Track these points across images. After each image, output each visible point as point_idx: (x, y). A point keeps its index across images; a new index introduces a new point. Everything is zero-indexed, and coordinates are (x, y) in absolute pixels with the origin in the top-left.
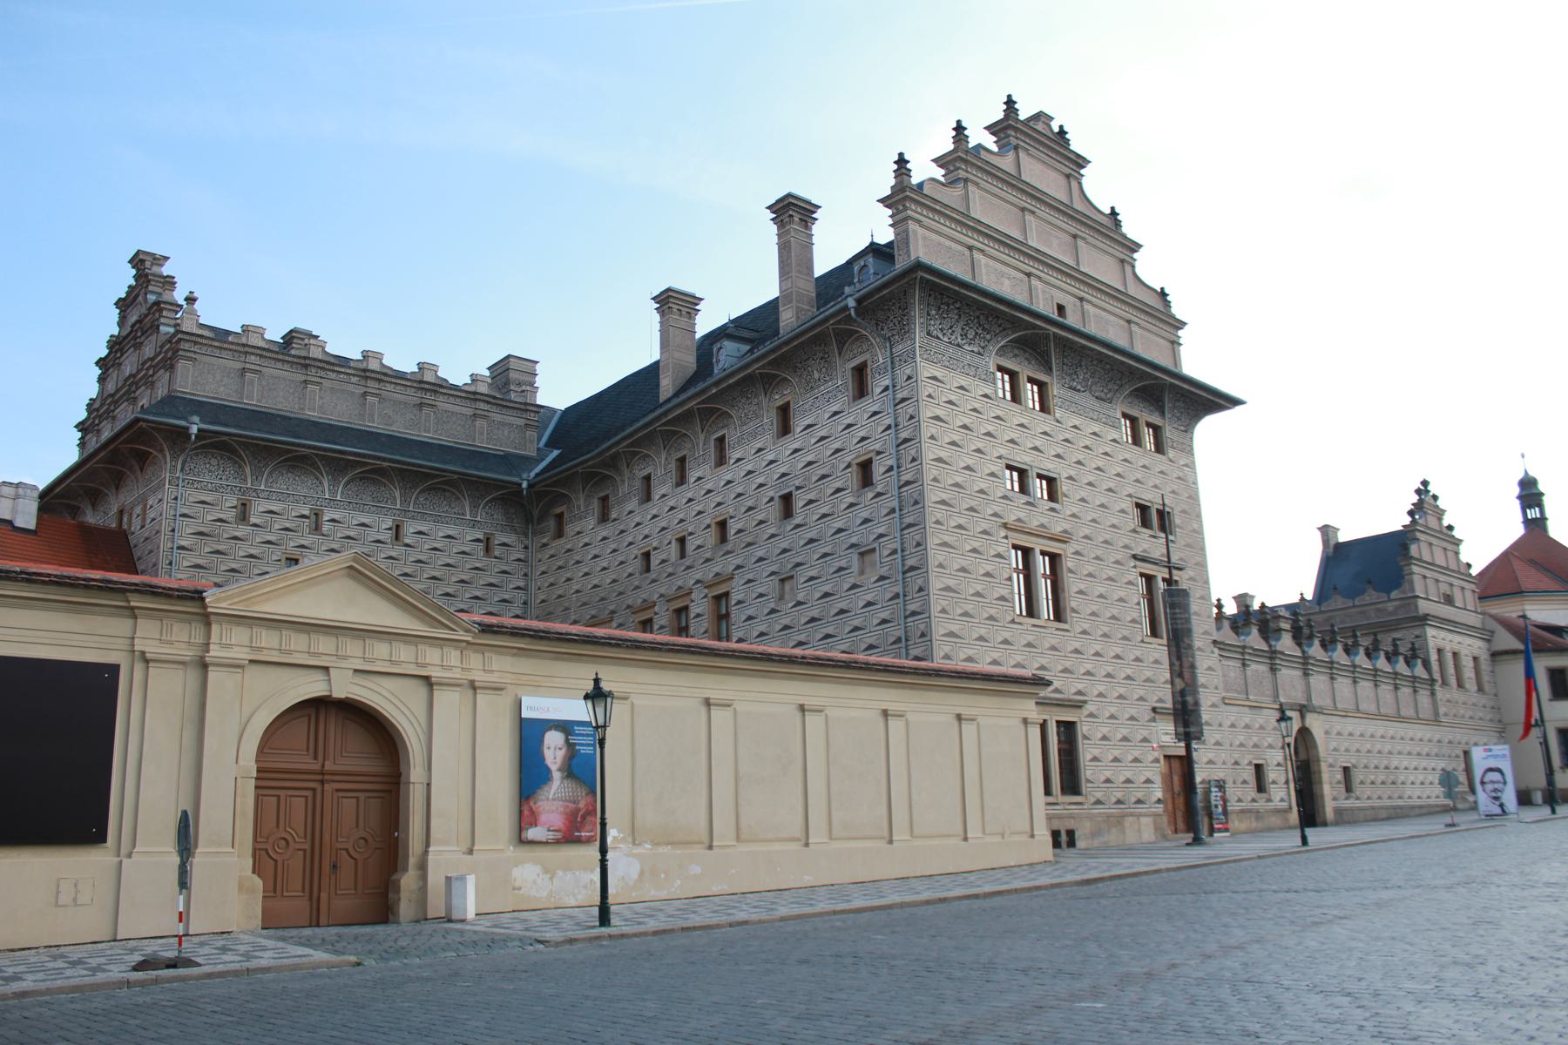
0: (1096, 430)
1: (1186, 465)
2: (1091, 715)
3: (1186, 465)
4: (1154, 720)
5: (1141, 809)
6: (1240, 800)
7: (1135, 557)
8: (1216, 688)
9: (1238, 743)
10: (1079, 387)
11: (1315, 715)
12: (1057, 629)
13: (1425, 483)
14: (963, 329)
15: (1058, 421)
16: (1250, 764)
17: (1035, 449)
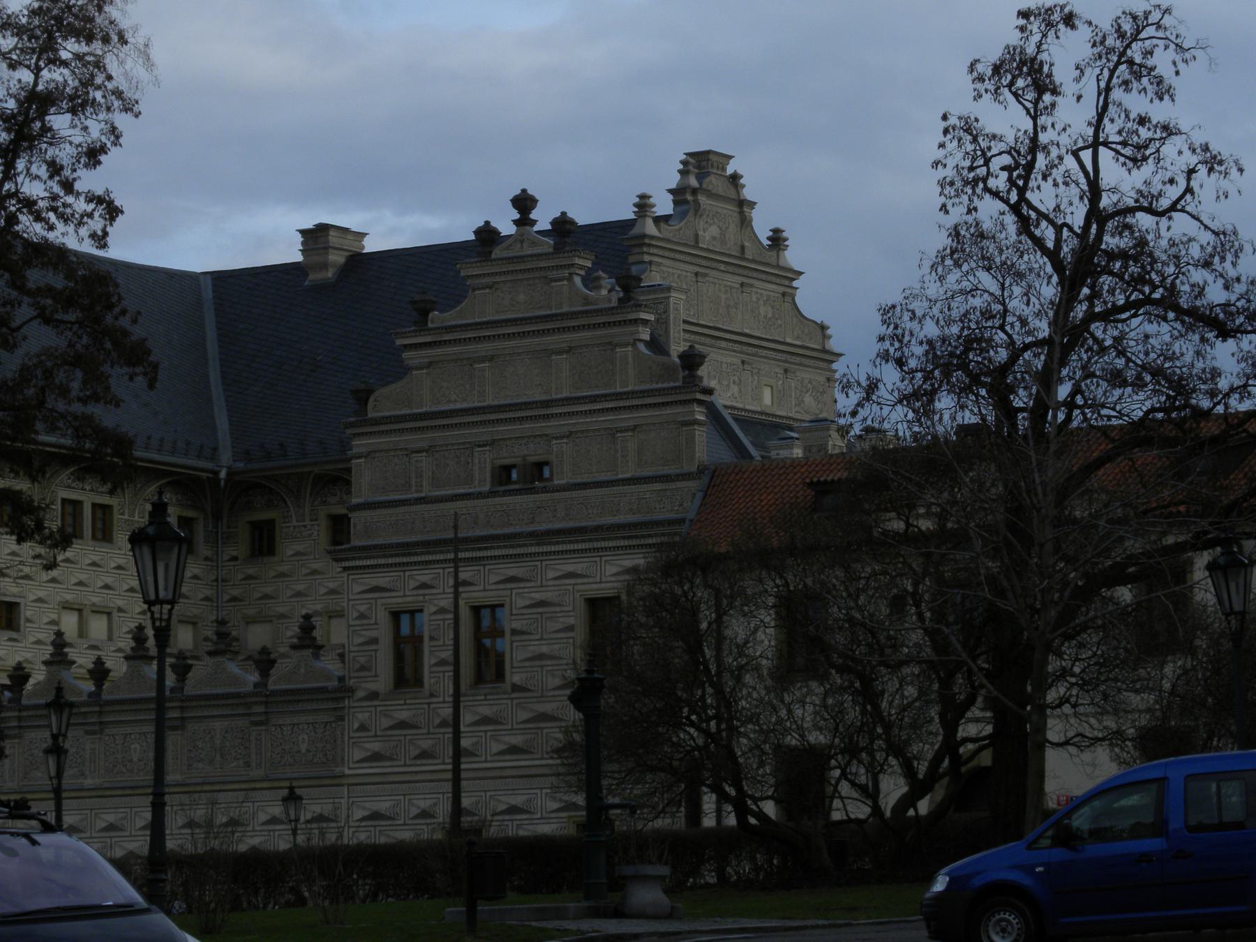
13: (524, 203)
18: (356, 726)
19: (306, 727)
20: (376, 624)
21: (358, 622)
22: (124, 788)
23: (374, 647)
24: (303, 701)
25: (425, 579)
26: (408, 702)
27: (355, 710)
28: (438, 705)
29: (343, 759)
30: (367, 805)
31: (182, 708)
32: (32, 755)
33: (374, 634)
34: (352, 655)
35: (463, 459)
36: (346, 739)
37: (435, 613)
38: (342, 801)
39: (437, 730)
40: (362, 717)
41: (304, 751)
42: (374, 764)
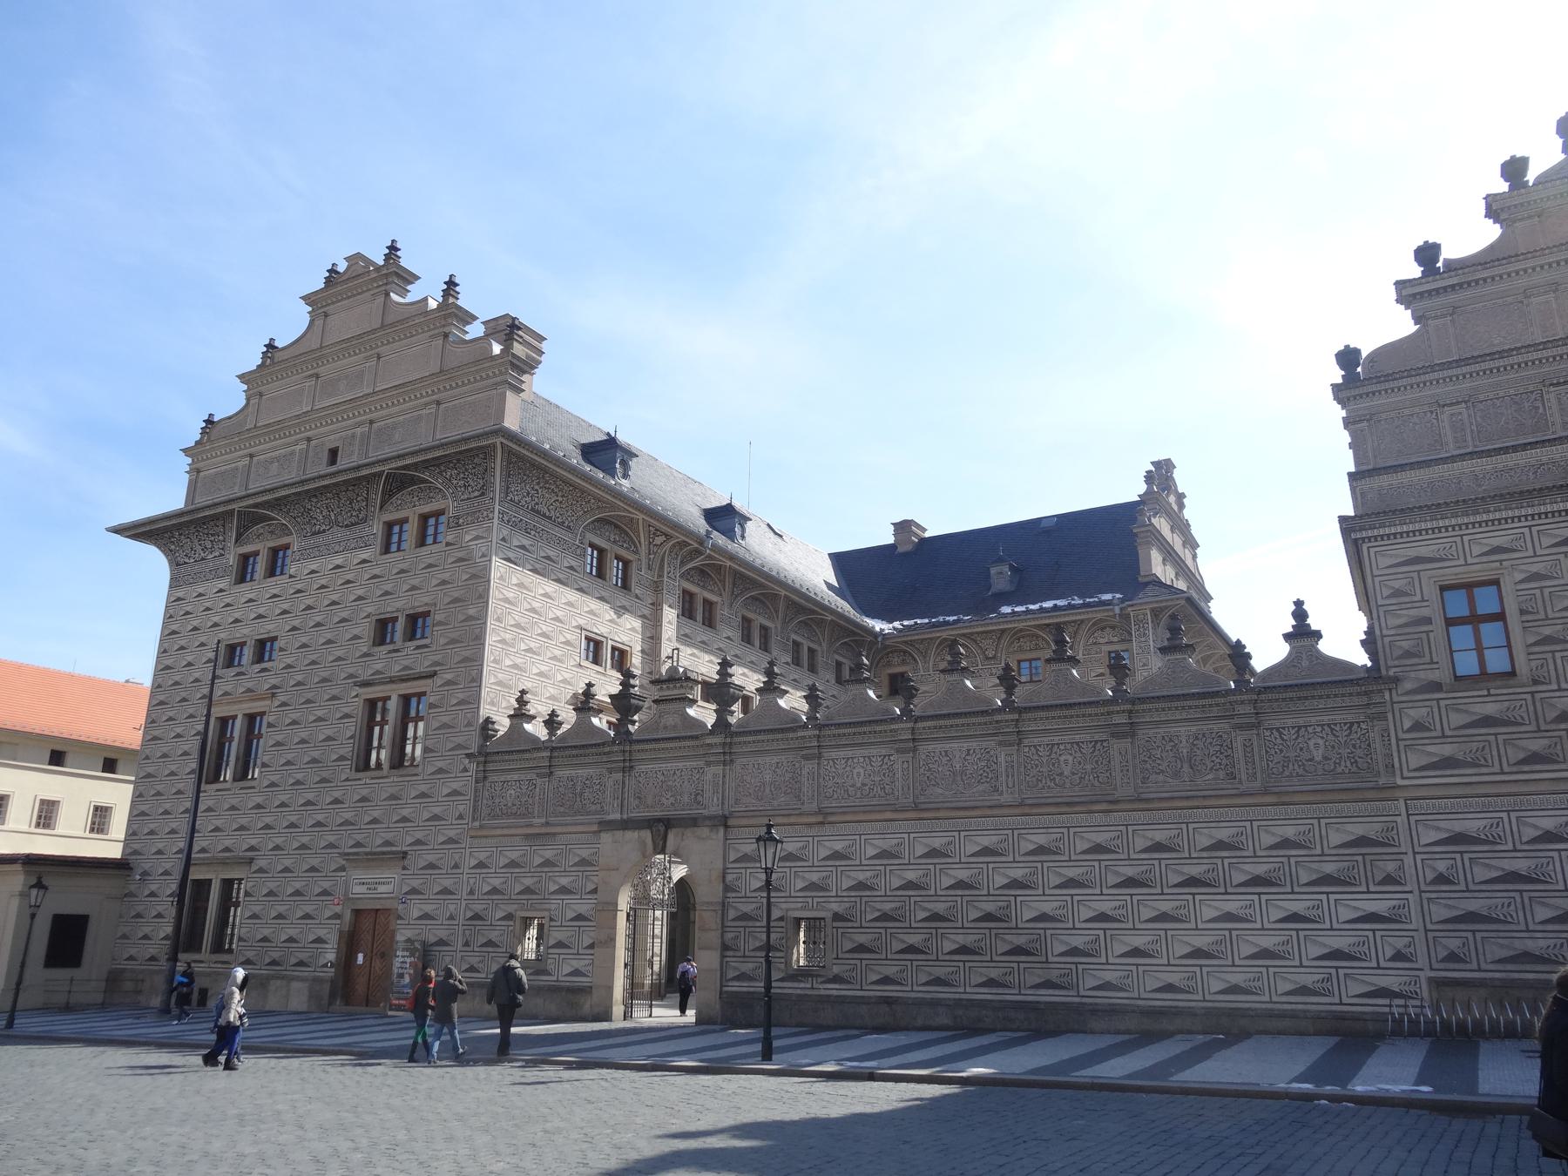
0: (339, 560)
1: (477, 538)
2: (261, 870)
3: (477, 538)
4: (342, 869)
5: (305, 972)
6: (472, 969)
7: (355, 684)
8: (461, 817)
9: (486, 888)
10: (324, 527)
11: (705, 831)
12: (241, 789)
14: (200, 545)
15: (291, 576)
16: (509, 917)
17: (260, 616)
18: (1407, 724)
19: (1319, 729)
20: (1423, 600)
21: (1394, 601)
22: (1057, 804)
23: (1429, 628)
24: (1313, 697)
25: (1496, 542)
26: (1492, 691)
27: (1404, 705)
28: (1548, 695)
29: (1390, 767)
30: (1442, 824)
31: (1130, 712)
32: (930, 769)
33: (1425, 612)
34: (1387, 640)
35: (1526, 405)
36: (1393, 741)
37: (1521, 582)
38: (1398, 819)
39: (1553, 727)
40: (1418, 713)
41: (1318, 758)
42: (1448, 772)
